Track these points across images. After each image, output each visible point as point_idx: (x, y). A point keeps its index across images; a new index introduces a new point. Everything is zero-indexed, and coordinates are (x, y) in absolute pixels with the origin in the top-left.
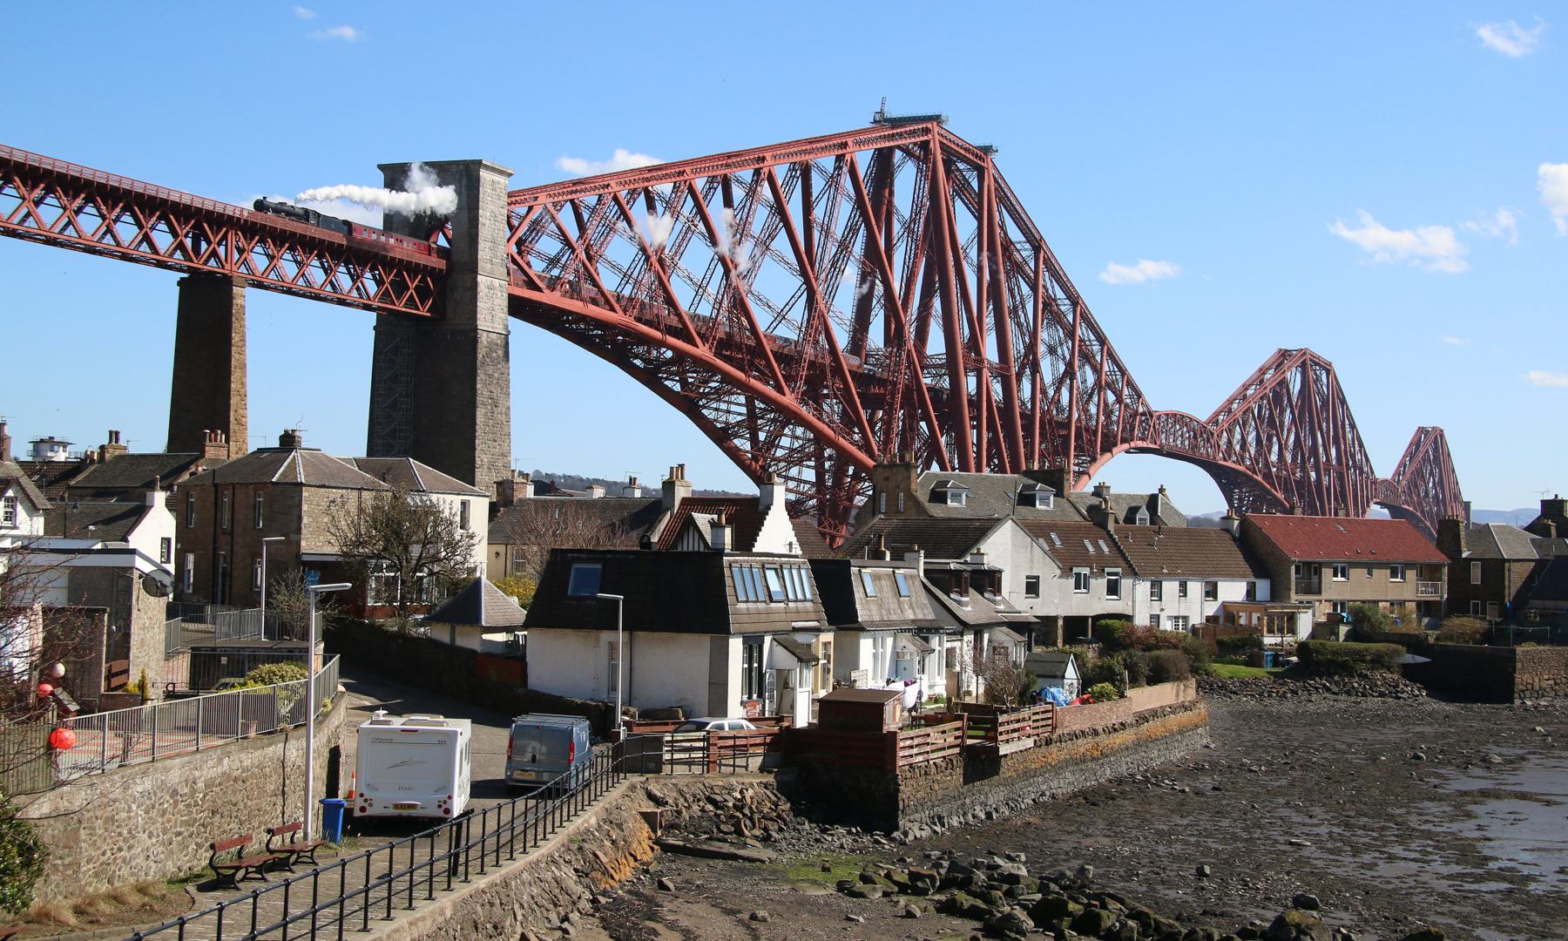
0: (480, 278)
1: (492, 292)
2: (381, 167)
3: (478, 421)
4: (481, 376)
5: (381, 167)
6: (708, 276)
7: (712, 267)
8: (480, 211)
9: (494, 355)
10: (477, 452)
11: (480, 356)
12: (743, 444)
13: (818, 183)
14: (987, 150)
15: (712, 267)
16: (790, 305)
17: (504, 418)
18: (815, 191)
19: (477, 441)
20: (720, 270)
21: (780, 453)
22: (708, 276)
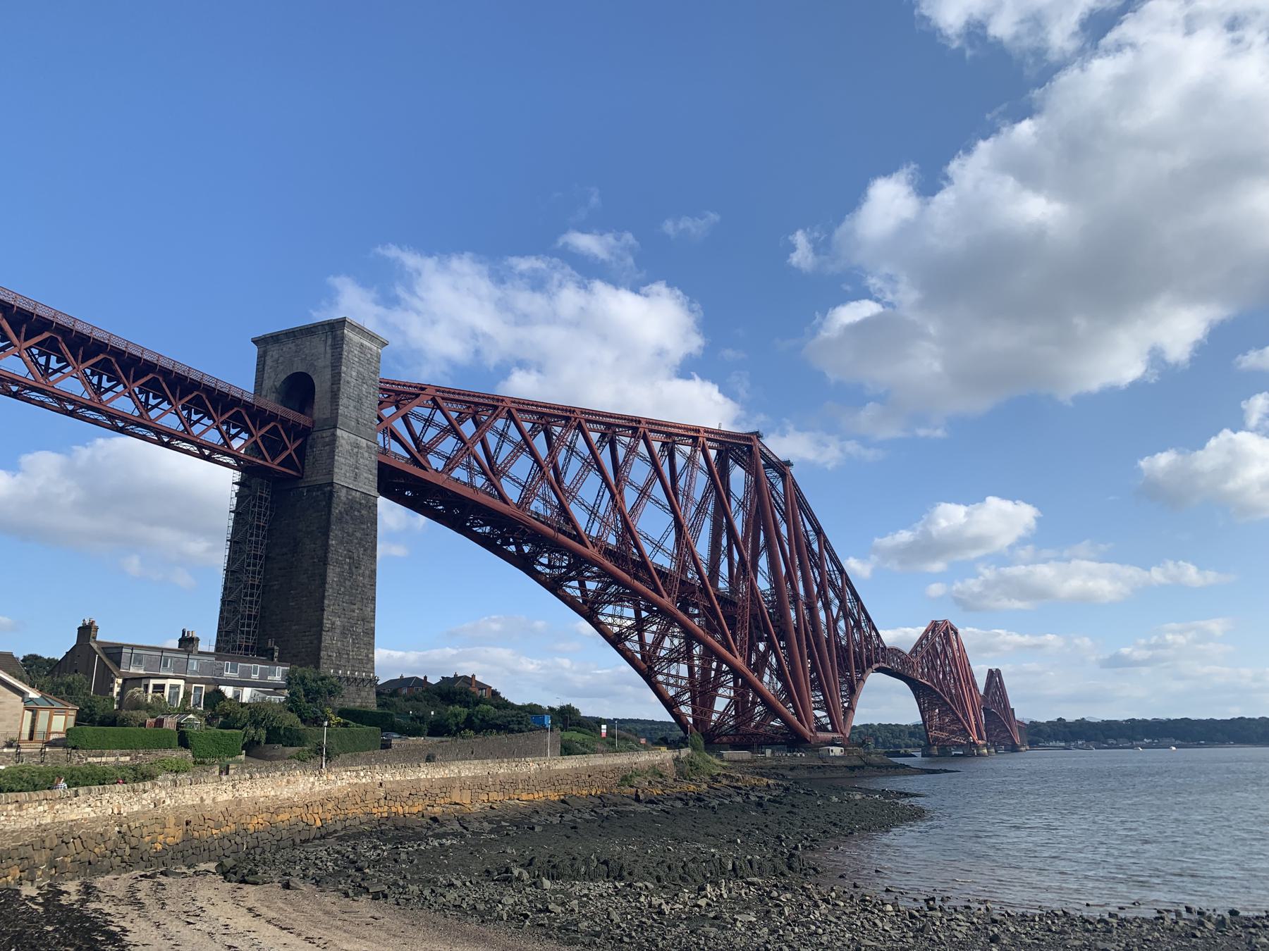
0: (339, 432)
1: (355, 450)
2: (255, 341)
3: (329, 580)
4: (335, 532)
5: (255, 341)
6: (598, 502)
7: (601, 494)
8: (344, 368)
9: (356, 513)
10: (325, 612)
11: (335, 511)
12: (630, 645)
13: (680, 461)
14: (788, 464)
15: (601, 494)
16: (665, 536)
17: (366, 581)
18: (678, 469)
19: (326, 602)
20: (607, 495)
21: (663, 653)
22: (598, 502)
